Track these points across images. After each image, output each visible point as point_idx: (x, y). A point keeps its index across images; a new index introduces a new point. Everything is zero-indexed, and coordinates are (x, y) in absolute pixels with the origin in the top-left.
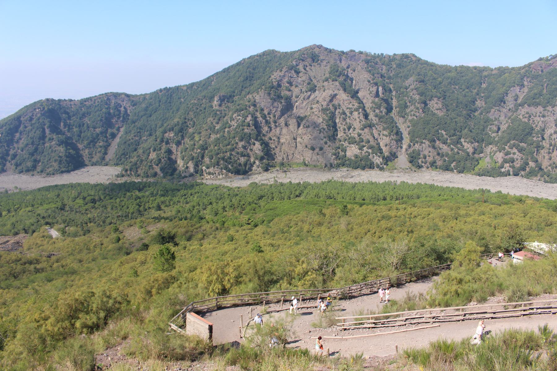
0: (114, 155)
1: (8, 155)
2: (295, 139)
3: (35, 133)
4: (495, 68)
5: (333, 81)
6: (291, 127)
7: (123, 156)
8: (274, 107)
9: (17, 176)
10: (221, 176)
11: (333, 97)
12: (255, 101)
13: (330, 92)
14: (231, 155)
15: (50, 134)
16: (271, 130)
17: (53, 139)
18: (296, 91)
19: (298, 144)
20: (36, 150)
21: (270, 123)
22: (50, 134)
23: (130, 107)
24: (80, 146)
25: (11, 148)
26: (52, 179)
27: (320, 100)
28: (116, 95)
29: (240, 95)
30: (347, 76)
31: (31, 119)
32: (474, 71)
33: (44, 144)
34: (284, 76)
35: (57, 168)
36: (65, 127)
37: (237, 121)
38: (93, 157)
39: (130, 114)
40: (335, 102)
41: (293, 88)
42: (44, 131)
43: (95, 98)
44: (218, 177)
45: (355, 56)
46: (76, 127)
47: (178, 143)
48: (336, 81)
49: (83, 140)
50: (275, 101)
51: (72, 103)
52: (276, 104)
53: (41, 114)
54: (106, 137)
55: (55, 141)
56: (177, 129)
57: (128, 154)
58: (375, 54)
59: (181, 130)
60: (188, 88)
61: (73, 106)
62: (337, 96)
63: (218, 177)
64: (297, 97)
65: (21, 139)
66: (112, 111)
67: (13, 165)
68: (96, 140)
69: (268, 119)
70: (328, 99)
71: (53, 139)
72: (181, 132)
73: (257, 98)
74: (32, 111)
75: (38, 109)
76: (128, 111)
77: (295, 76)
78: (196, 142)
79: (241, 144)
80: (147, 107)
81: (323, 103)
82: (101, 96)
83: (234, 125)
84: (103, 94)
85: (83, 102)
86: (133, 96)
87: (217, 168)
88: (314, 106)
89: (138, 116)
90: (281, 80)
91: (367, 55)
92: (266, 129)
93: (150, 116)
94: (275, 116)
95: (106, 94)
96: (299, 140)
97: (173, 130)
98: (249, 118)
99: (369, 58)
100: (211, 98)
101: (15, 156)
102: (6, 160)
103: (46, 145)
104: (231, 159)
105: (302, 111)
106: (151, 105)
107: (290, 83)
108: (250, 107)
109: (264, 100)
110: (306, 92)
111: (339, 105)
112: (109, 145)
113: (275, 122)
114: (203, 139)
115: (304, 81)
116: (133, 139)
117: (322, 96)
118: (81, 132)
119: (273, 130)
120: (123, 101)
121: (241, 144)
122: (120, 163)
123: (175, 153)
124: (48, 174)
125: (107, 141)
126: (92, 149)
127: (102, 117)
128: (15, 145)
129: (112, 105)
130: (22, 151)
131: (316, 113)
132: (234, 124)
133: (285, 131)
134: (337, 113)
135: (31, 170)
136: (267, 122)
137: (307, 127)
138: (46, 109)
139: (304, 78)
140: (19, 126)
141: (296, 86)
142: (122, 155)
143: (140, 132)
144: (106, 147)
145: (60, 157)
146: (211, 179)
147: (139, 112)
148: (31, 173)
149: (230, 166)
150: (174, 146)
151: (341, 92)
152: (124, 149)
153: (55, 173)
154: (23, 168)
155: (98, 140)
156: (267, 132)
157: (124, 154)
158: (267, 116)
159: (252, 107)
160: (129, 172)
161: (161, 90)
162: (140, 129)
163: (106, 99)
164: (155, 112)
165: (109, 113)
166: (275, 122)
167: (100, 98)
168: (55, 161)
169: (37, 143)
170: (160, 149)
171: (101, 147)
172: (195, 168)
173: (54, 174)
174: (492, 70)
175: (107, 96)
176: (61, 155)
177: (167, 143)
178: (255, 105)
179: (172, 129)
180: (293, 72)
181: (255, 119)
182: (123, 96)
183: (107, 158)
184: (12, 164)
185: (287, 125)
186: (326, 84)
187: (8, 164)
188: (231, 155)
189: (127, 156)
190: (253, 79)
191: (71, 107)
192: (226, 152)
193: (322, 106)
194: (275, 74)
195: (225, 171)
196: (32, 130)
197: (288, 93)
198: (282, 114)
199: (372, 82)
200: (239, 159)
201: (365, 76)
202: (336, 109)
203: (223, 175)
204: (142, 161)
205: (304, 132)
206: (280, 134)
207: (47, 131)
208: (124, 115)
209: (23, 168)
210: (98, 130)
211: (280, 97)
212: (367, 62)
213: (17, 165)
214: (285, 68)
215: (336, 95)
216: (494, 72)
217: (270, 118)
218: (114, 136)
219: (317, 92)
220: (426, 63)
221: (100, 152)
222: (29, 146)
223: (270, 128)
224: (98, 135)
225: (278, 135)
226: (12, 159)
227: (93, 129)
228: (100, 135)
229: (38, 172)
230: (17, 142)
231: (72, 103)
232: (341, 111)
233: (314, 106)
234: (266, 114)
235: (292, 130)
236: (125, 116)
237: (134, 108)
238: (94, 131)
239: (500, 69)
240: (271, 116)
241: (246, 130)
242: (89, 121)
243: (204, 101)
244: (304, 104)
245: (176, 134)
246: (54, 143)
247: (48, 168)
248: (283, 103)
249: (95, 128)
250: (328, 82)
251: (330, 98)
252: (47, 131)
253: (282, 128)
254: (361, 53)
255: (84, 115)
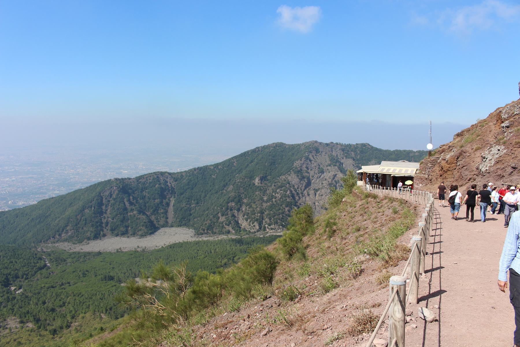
0: (175, 219)
1: (102, 223)
2: (315, 203)
3: (119, 205)
4: (417, 151)
5: (334, 166)
6: (311, 196)
7: (183, 220)
8: (301, 184)
9: (118, 238)
10: (279, 230)
11: (335, 176)
12: (288, 181)
13: (333, 173)
14: (283, 216)
15: (130, 206)
16: (300, 199)
17: (133, 209)
18: (312, 173)
19: (317, 207)
20: (124, 217)
21: (299, 194)
22: (130, 206)
23: (173, 182)
24: (148, 213)
25: (102, 217)
26: (146, 239)
27: (327, 178)
28: (162, 174)
29: (271, 175)
30: (340, 162)
31: (111, 195)
32: (404, 153)
33: (127, 213)
34: (304, 163)
35: (146, 231)
36: (134, 200)
37: (281, 194)
38: (159, 221)
39: (175, 188)
40: (336, 179)
41: (309, 171)
42: (124, 203)
43: (146, 176)
44: (278, 231)
45: (334, 146)
46: (140, 199)
47: (239, 210)
48: (336, 166)
49: (148, 209)
50: (302, 180)
51: (131, 181)
52: (302, 182)
53: (118, 191)
54: (163, 205)
55: (135, 211)
56: (236, 200)
57: (186, 218)
58: (345, 144)
59: (239, 201)
60: (214, 168)
61: (132, 183)
62: (337, 175)
63: (278, 231)
64: (313, 177)
65: (107, 210)
66: (163, 186)
67: (109, 230)
68: (157, 209)
69: (298, 191)
70: (332, 177)
71: (133, 209)
72: (239, 202)
73: (289, 178)
74: (110, 189)
75: (116, 187)
76: (173, 185)
77: (310, 163)
78: (255, 209)
79: (287, 209)
80: (189, 182)
81: (329, 180)
82: (151, 175)
83: (278, 197)
84: (151, 173)
85: (139, 178)
86: (174, 174)
87: (277, 225)
88: (324, 182)
89: (183, 189)
90: (301, 166)
91: (341, 145)
92: (297, 198)
93: (193, 189)
94: (301, 190)
95: (154, 173)
96: (316, 204)
97: (234, 201)
98: (288, 192)
99: (343, 147)
100: (252, 178)
101: (107, 223)
102: (103, 227)
103: (129, 214)
104: (283, 219)
105: (316, 185)
106: (191, 181)
107: (307, 168)
108: (286, 185)
109: (295, 180)
110: (319, 173)
111: (338, 181)
112: (167, 211)
113: (302, 193)
114: (259, 207)
115: (316, 167)
116: (186, 207)
117: (327, 176)
118: (145, 203)
119: (301, 199)
120: (167, 178)
121: (287, 209)
122: (182, 224)
123: (237, 216)
124: (142, 236)
125: (165, 209)
126: (157, 215)
127: (159, 191)
128: (104, 215)
129: (162, 181)
130: (113, 219)
131: (326, 186)
132: (278, 196)
133: (307, 199)
134: (337, 186)
135: (125, 233)
136: (298, 194)
137: (321, 196)
138: (121, 187)
139: (315, 164)
140: (102, 200)
141: (311, 170)
142: (182, 219)
143: (188, 201)
144: (166, 212)
145: (145, 222)
146: (273, 232)
147: (183, 186)
148: (126, 236)
149: (283, 223)
150: (236, 211)
151: (339, 172)
152: (182, 215)
153: (146, 235)
154: (118, 233)
155: (159, 208)
156: (298, 200)
157: (183, 218)
158: (297, 190)
159: (288, 185)
160: (206, 231)
161: (195, 169)
162: (189, 199)
163: (156, 177)
164: (195, 186)
165: (162, 188)
166: (302, 193)
167: (150, 176)
168: (143, 226)
169: (123, 213)
170: (227, 214)
171: (163, 213)
172: (259, 226)
173: (146, 236)
174: (414, 152)
175: (156, 174)
176: (144, 221)
177: (231, 210)
178: (289, 183)
179: (232, 201)
180: (308, 161)
181: (291, 191)
182: (167, 174)
183: (170, 221)
184: (107, 230)
185: (308, 195)
186: (329, 168)
187: (105, 230)
188: (283, 216)
189: (186, 219)
190: (275, 163)
191: (132, 184)
192: (280, 214)
193: (329, 181)
194: (297, 162)
195: (281, 227)
196: (115, 203)
197: (307, 174)
198: (305, 188)
199: (355, 165)
200: (287, 219)
201: (350, 162)
202: (337, 183)
203: (280, 229)
204: (214, 223)
205: (320, 199)
206: (305, 201)
207: (127, 204)
208: (172, 189)
209: (118, 233)
210: (157, 201)
211: (304, 177)
212: (343, 150)
213: (112, 230)
214: (303, 158)
215: (336, 175)
216: (416, 154)
217: (299, 191)
218: (168, 205)
219: (325, 173)
220: (377, 149)
221: (163, 217)
222: (119, 216)
223: (299, 197)
224: (158, 204)
225: (304, 201)
226: (107, 225)
227: (153, 201)
228: (160, 205)
229: (131, 235)
230: (106, 213)
231: (131, 181)
232: (340, 185)
233: (324, 182)
234: (296, 188)
235: (312, 198)
236: (172, 189)
237: (176, 183)
238: (154, 201)
239: (419, 152)
240: (299, 190)
241: (288, 200)
242: (148, 194)
243: (246, 179)
244: (318, 181)
245: (236, 204)
246: (135, 212)
247: (138, 231)
248: (306, 181)
249: (154, 199)
250: (331, 167)
251: (333, 177)
252: (127, 204)
253: (306, 197)
254: (337, 144)
255: (142, 190)
